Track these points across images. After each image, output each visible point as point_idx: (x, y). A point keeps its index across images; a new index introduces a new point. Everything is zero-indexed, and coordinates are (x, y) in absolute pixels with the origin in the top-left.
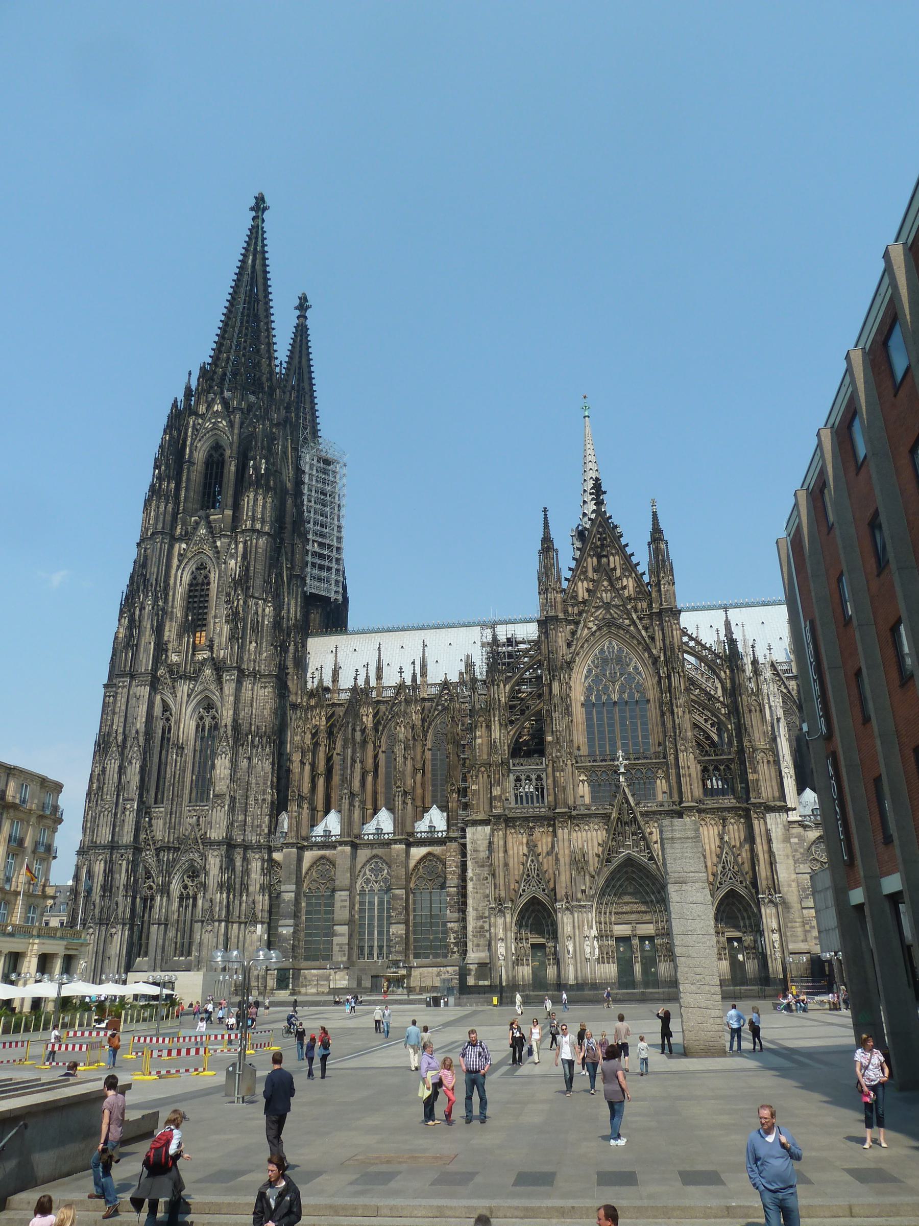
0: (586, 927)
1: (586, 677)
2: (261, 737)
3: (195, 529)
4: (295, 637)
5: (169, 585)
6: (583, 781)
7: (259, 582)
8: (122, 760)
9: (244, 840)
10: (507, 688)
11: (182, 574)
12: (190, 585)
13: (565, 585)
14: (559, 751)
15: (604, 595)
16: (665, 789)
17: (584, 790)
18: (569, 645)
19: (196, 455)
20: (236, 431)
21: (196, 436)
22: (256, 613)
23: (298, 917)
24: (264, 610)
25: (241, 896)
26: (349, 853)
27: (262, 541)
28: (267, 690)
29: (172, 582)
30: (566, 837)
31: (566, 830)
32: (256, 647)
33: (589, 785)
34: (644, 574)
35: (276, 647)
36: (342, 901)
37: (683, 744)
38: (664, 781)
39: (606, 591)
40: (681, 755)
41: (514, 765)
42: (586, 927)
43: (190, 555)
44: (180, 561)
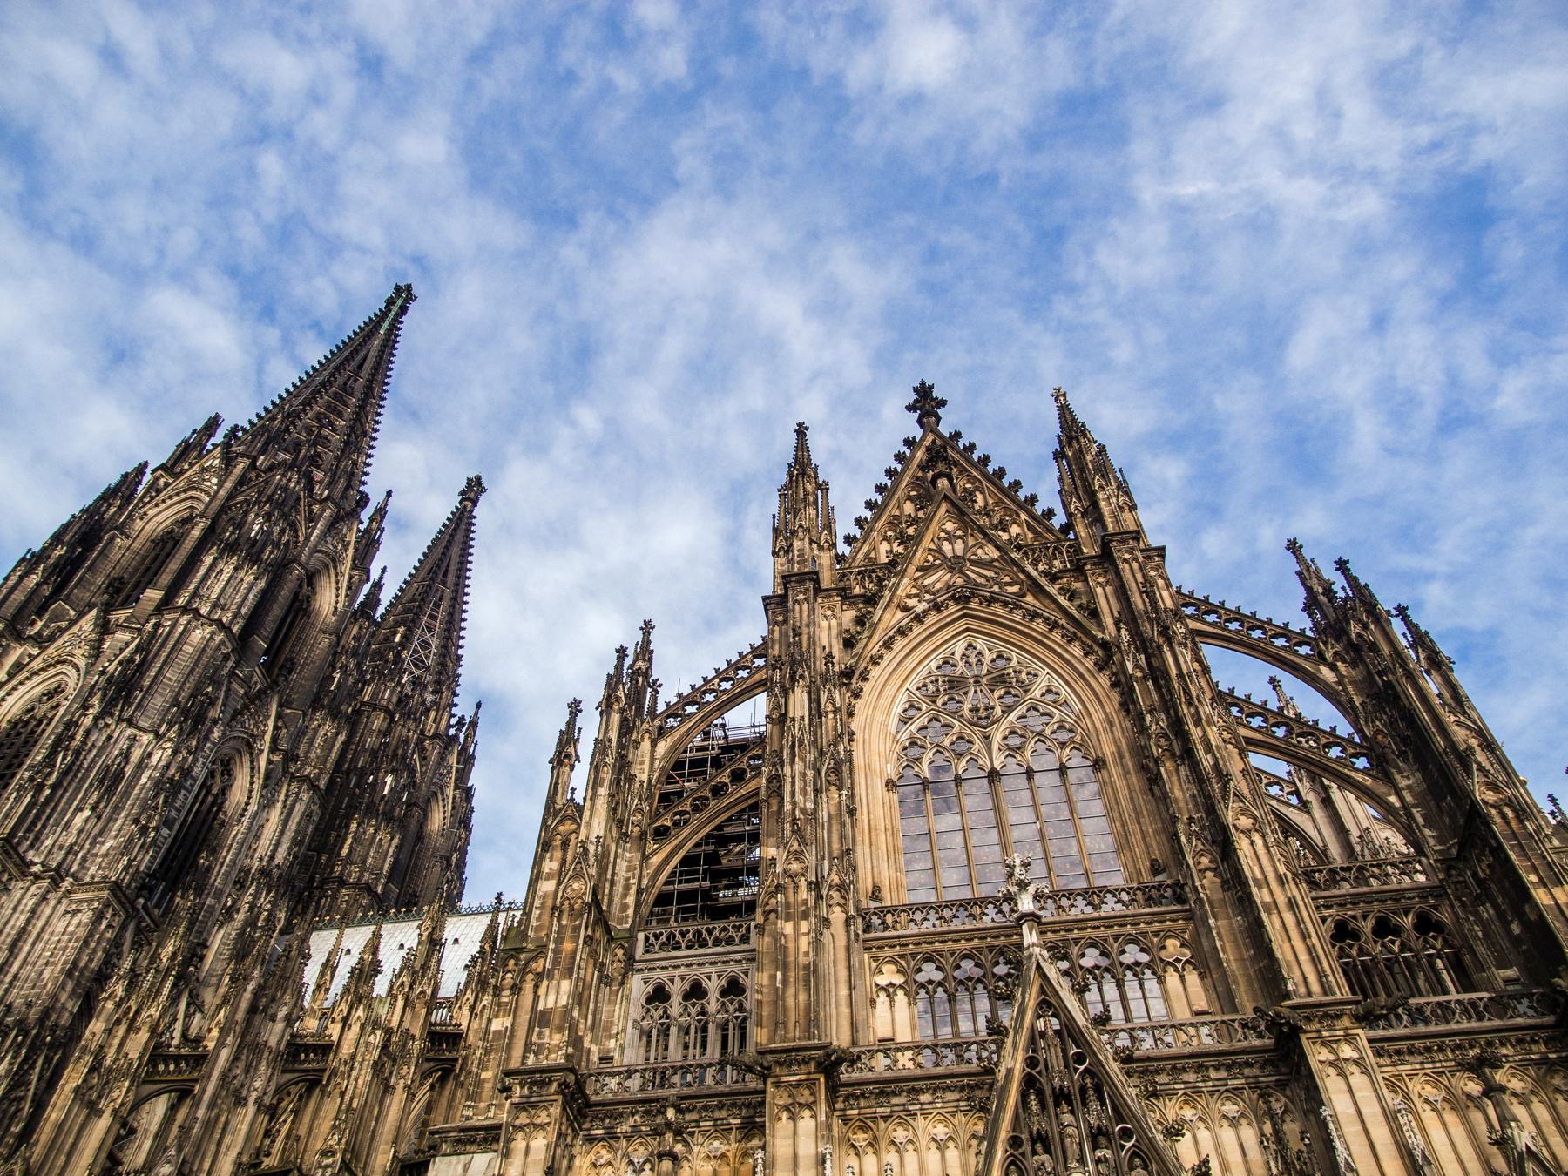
1: (904, 721)
3: (73, 623)
4: (256, 896)
6: (889, 990)
7: (158, 702)
10: (662, 747)
12: (14, 724)
13: (843, 548)
14: (798, 856)
15: (946, 547)
16: (1202, 1005)
17: (895, 1019)
18: (849, 644)
19: (139, 524)
21: (152, 498)
22: (126, 755)
24: (150, 755)
27: (198, 635)
28: (75, 921)
30: (807, 1148)
31: (807, 1123)
32: (87, 820)
33: (912, 999)
34: (1049, 513)
35: (144, 830)
37: (1244, 812)
38: (1192, 978)
39: (950, 538)
40: (1243, 846)
43: (37, 664)
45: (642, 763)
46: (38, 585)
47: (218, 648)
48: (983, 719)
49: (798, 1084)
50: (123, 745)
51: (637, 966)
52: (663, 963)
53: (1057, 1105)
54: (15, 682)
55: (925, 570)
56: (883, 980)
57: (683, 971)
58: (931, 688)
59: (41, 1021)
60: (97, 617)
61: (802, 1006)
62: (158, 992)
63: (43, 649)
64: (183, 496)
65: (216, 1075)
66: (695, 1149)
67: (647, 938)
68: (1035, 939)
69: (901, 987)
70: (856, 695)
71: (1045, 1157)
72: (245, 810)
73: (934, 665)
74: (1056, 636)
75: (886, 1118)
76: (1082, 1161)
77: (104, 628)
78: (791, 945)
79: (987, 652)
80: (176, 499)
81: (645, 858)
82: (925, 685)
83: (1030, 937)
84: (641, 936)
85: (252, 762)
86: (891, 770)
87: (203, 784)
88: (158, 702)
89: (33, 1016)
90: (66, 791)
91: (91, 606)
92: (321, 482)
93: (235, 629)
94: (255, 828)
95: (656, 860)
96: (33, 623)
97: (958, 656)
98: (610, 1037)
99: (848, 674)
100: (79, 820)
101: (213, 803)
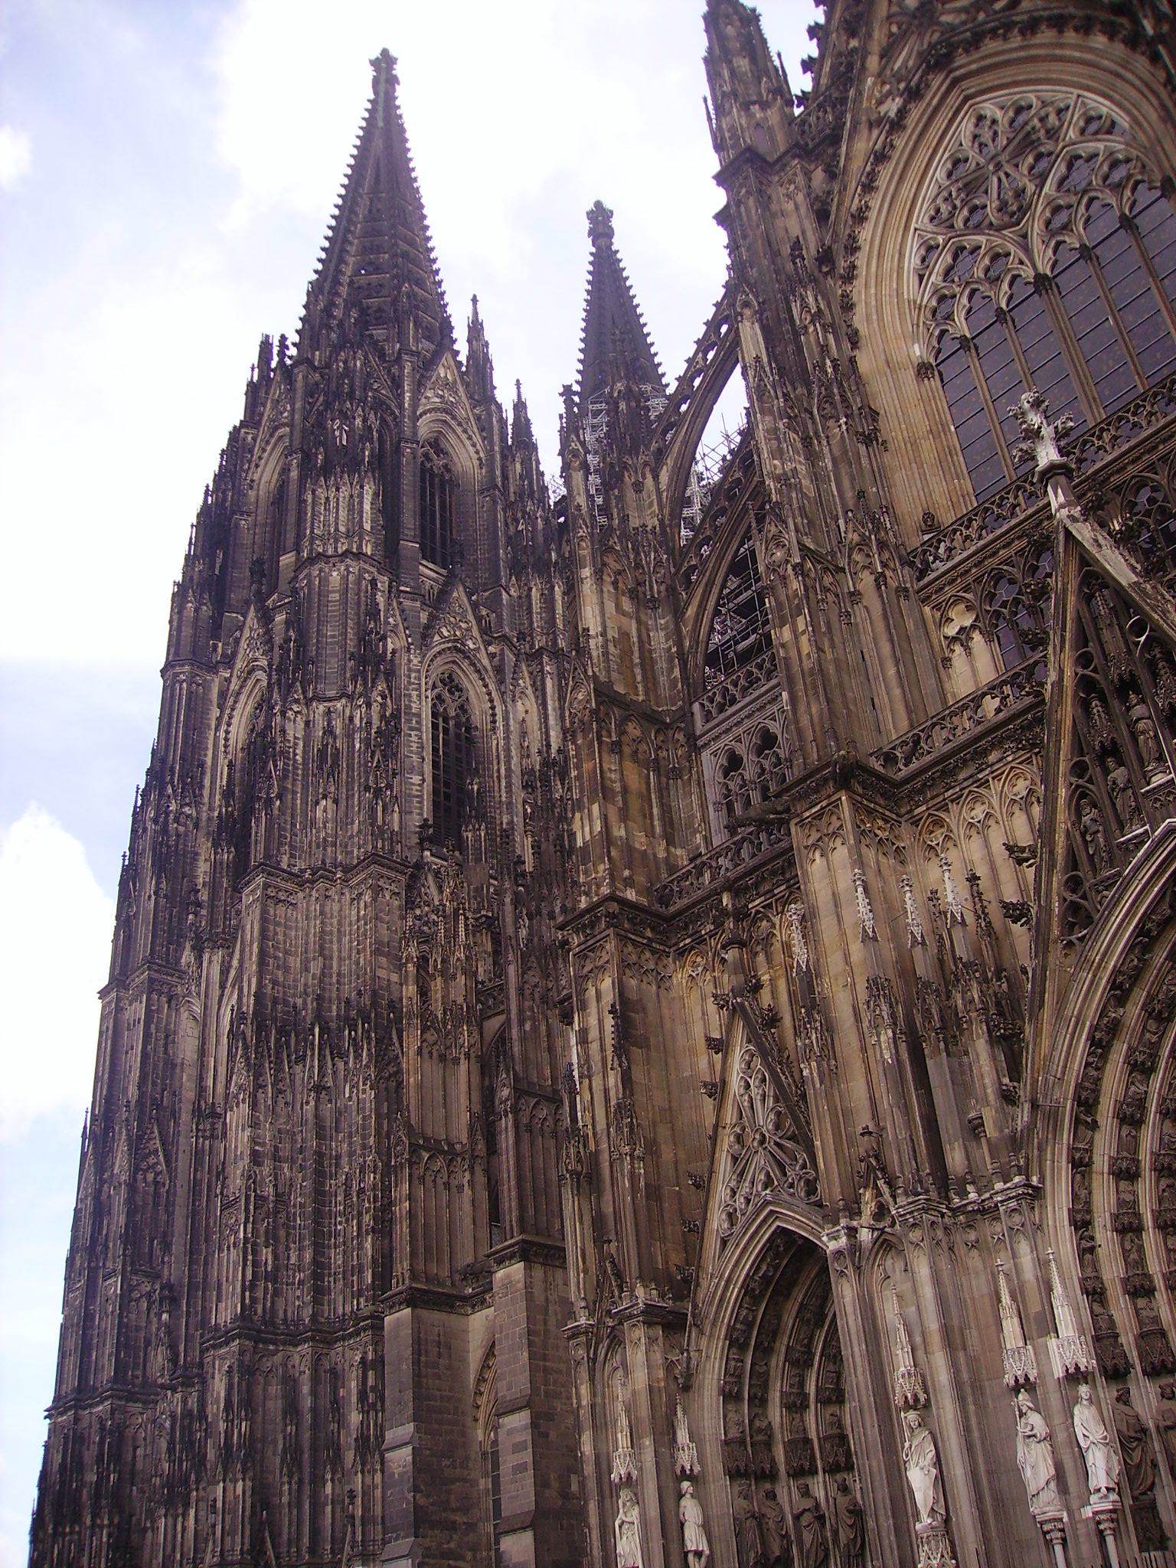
0: (1011, 1327)
2: (353, 1027)
5: (202, 765)
6: (963, 637)
8: (102, 1182)
9: (314, 1317)
11: (227, 732)
20: (298, 405)
21: (249, 462)
22: (329, 731)
23: (452, 1526)
24: (351, 719)
25: (317, 1481)
26: (521, 1285)
29: (209, 760)
30: (845, 878)
31: (841, 854)
33: (989, 636)
36: (519, 1447)
41: (708, 717)
42: (1011, 1327)
44: (221, 707)
45: (651, 505)
46: (197, 610)
47: (360, 578)
48: (1016, 211)
49: (819, 816)
50: (320, 723)
51: (700, 743)
52: (723, 727)
53: (1124, 699)
54: (228, 711)
55: (887, 54)
56: (951, 630)
57: (747, 724)
58: (945, 209)
59: (374, 1004)
60: (257, 611)
61: (816, 720)
62: (456, 935)
63: (231, 668)
64: (273, 441)
65: (513, 993)
66: (776, 920)
67: (702, 705)
68: (1061, 499)
69: (973, 627)
70: (849, 277)
71: (1119, 774)
72: (494, 715)
73: (940, 175)
74: (1071, 36)
75: (955, 800)
76: (1161, 759)
77: (266, 618)
78: (793, 653)
79: (999, 114)
80: (269, 448)
81: (678, 614)
82: (938, 211)
83: (1056, 498)
84: (696, 707)
85: (473, 664)
86: (918, 351)
87: (434, 715)
88: (331, 666)
89: (366, 1000)
90: (294, 793)
91: (247, 603)
92: (387, 340)
93: (368, 550)
94: (513, 726)
95: (691, 612)
96: (215, 647)
97: (966, 143)
98: (695, 832)
99: (826, 257)
100: (319, 813)
101: (458, 725)
